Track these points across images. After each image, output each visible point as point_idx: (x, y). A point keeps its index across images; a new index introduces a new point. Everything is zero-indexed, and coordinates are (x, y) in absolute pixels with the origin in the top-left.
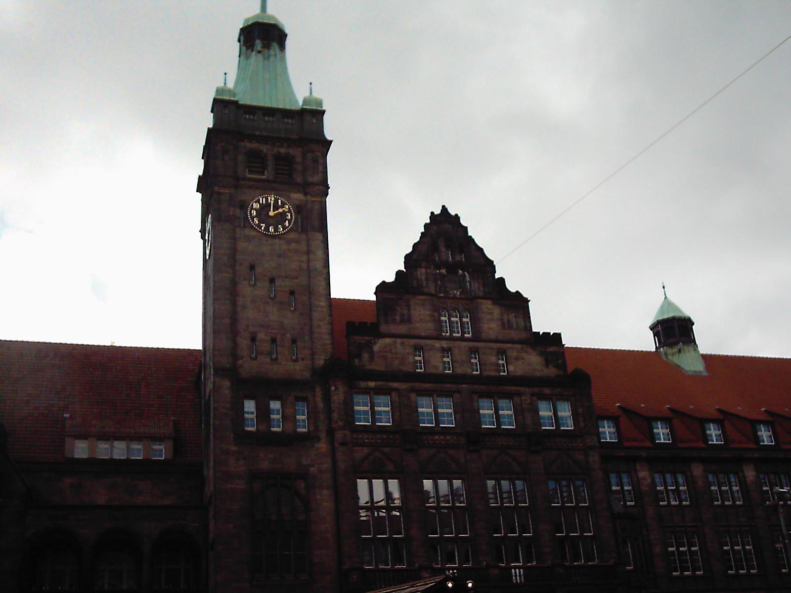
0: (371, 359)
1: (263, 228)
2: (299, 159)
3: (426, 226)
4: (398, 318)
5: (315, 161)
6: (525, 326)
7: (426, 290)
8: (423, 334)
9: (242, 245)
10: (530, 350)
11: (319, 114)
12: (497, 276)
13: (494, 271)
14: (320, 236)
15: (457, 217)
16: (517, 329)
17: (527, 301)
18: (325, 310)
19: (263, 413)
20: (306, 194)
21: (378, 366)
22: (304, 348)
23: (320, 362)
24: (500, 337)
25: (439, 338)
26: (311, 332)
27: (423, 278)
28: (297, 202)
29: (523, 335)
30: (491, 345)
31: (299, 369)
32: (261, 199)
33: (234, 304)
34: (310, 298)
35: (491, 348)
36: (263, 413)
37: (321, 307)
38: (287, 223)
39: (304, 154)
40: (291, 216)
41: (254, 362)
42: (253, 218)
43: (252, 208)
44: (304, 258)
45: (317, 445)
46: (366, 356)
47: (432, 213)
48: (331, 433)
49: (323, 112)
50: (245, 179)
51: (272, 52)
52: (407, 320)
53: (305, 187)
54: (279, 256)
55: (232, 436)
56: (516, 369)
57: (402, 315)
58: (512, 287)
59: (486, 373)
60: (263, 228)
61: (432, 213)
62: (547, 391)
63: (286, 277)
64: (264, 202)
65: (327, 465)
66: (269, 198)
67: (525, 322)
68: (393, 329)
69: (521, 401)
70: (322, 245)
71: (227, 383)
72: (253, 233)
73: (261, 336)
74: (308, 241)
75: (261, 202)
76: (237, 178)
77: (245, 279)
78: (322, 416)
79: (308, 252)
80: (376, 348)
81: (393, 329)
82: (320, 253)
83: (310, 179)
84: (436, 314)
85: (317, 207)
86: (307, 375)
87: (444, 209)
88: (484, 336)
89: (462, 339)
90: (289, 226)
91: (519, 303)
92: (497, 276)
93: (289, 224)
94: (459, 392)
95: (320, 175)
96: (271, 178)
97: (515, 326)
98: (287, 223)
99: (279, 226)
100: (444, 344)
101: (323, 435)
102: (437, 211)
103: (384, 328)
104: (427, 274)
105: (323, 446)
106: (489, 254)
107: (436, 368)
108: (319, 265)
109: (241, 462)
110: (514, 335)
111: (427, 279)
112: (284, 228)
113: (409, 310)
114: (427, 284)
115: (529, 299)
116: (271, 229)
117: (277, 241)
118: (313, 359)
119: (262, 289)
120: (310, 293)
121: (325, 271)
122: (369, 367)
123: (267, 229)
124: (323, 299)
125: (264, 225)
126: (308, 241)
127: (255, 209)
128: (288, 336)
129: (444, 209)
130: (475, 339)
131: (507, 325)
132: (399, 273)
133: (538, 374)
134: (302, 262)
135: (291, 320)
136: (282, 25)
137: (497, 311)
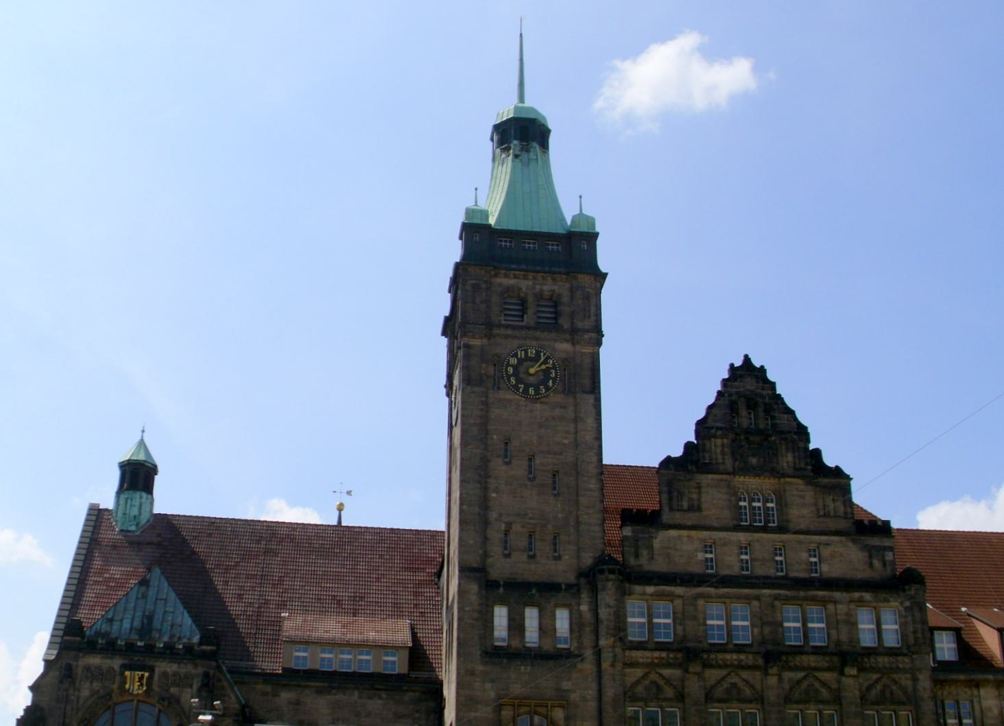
0: (652, 558)
1: (521, 390)
2: (565, 299)
3: (725, 382)
4: (685, 505)
5: (587, 297)
6: (846, 513)
8: (716, 524)
9: (495, 412)
10: (850, 544)
11: (592, 237)
12: (812, 446)
13: (807, 439)
14: (590, 399)
15: (762, 370)
16: (835, 516)
17: (848, 478)
18: (595, 494)
19: (517, 626)
20: (573, 344)
21: (660, 565)
22: (569, 543)
23: (588, 560)
24: (812, 528)
25: (737, 528)
26: (578, 523)
27: (719, 450)
28: (563, 355)
29: (843, 524)
30: (802, 537)
32: (519, 352)
33: (485, 489)
34: (577, 480)
35: (800, 542)
36: (517, 626)
37: (591, 490)
38: (550, 383)
39: (572, 290)
40: (556, 373)
41: (508, 560)
42: (509, 377)
43: (508, 365)
44: (571, 427)
45: (579, 666)
46: (645, 552)
47: (732, 365)
48: (598, 652)
49: (596, 235)
50: (500, 326)
51: (532, 155)
52: (696, 508)
53: (574, 334)
54: (541, 426)
55: (479, 653)
56: (828, 570)
57: (691, 499)
58: (829, 460)
59: (793, 574)
60: (521, 390)
61: (732, 365)
62: (867, 596)
63: (549, 452)
64: (523, 356)
65: (592, 692)
66: (529, 350)
67: (845, 506)
68: (678, 517)
69: (836, 609)
70: (593, 411)
72: (509, 396)
73: (517, 528)
74: (576, 406)
75: (519, 356)
76: (490, 325)
77: (499, 456)
78: (588, 629)
79: (576, 420)
80: (657, 543)
81: (678, 517)
82: (590, 421)
83: (580, 325)
84: (733, 498)
85: (588, 361)
86: (571, 578)
87: (747, 359)
89: (765, 529)
90: (553, 386)
91: (838, 481)
92: (812, 446)
93: (553, 383)
94: (758, 598)
95: (593, 318)
96: (532, 323)
97: (832, 513)
98: (550, 383)
99: (541, 387)
100: (742, 537)
101: (589, 653)
102: (738, 363)
103: (666, 517)
104: (723, 445)
105: (588, 666)
106: (802, 418)
108: (589, 437)
109: (488, 686)
111: (723, 453)
112: (547, 389)
113: (700, 493)
114: (724, 459)
115: (851, 477)
116: (531, 391)
117: (538, 406)
118: (578, 557)
119: (519, 468)
120: (577, 473)
121: (596, 444)
122: (647, 567)
123: (526, 391)
124: (594, 481)
125: (522, 386)
126: (576, 406)
127: (512, 366)
128: (550, 527)
129: (747, 359)
130: (781, 529)
132: (688, 446)
133: (859, 575)
134: (568, 432)
136: (544, 118)
137: (809, 494)
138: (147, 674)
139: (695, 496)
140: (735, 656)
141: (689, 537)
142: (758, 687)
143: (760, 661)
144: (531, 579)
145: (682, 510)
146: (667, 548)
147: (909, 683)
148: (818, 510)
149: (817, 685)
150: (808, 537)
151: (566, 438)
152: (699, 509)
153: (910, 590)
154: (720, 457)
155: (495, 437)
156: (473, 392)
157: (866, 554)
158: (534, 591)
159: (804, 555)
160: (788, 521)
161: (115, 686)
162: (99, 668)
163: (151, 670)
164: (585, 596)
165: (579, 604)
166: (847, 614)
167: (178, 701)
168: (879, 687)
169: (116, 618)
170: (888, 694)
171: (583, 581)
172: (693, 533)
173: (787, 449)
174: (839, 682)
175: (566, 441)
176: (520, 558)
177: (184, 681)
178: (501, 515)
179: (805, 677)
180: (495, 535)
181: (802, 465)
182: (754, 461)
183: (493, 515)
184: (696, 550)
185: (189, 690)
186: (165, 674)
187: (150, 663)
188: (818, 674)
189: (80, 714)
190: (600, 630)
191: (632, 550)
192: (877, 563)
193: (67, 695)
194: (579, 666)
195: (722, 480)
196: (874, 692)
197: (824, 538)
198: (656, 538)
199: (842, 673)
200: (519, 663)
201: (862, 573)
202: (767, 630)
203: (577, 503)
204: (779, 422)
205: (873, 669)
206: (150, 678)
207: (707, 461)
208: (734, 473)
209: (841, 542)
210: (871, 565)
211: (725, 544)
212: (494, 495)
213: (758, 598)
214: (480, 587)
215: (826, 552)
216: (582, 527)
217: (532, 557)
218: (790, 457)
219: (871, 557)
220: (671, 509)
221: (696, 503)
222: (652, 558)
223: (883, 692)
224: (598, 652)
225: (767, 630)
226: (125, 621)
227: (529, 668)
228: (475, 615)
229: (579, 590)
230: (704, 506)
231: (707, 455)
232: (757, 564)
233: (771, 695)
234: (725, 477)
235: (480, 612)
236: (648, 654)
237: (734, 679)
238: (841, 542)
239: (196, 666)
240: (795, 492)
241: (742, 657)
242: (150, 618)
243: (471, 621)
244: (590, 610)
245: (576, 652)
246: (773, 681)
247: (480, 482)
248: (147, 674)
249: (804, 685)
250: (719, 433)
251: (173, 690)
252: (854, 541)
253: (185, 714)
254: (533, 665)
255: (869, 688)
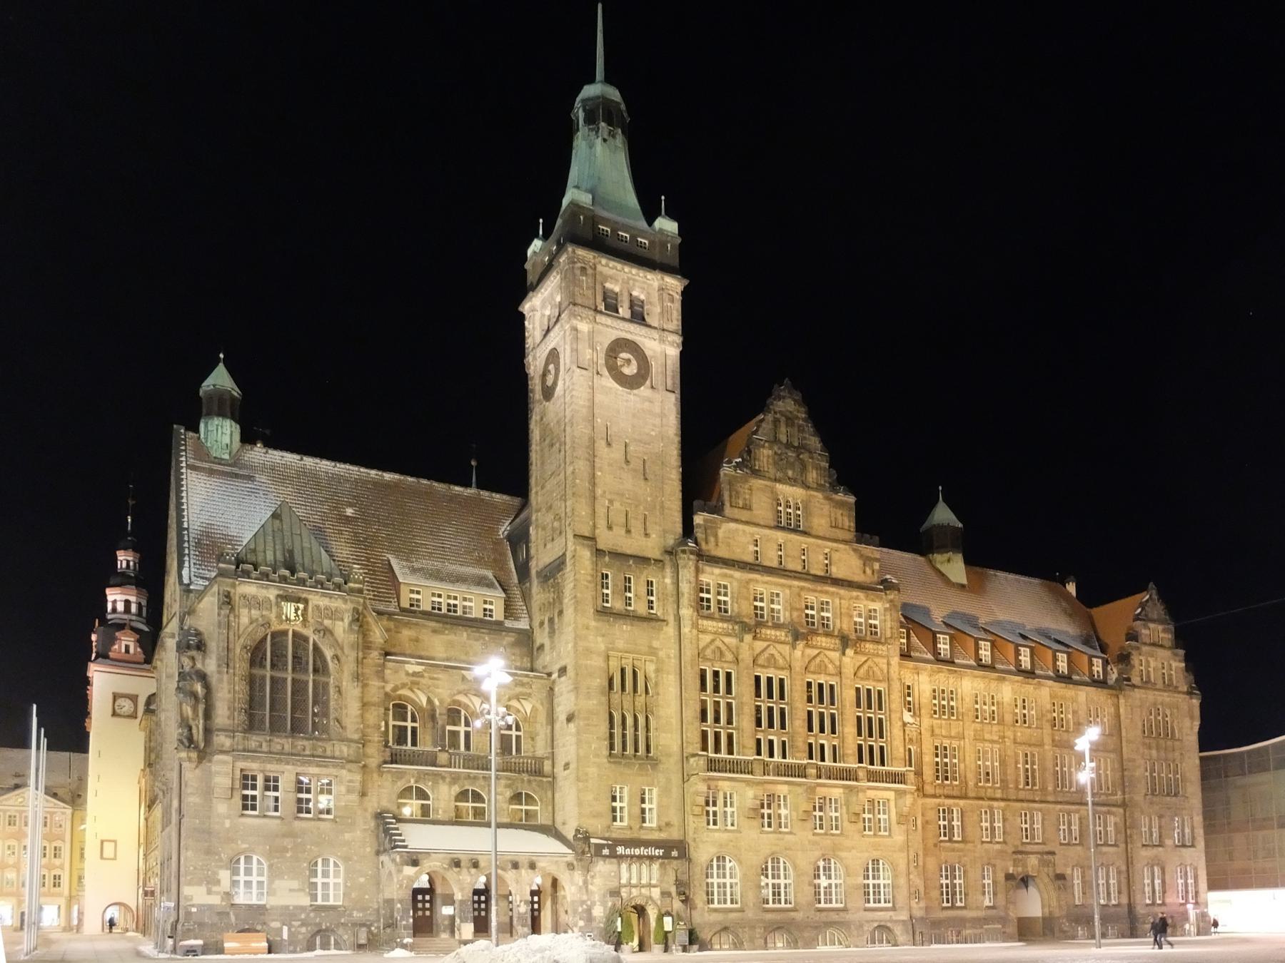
4: (741, 503)
7: (767, 475)
8: (762, 523)
9: (599, 398)
16: (842, 529)
21: (722, 552)
24: (828, 536)
26: (662, 507)
27: (765, 460)
30: (820, 542)
31: (651, 546)
35: (818, 546)
37: (672, 480)
41: (611, 533)
46: (712, 539)
52: (747, 507)
57: (745, 499)
71: (586, 554)
73: (617, 505)
78: (671, 599)
80: (721, 533)
81: (736, 513)
86: (655, 553)
88: (814, 533)
97: (840, 526)
100: (781, 536)
101: (671, 619)
103: (728, 510)
107: (771, 560)
110: (840, 534)
113: (751, 494)
119: (617, 454)
130: (805, 533)
131: (834, 525)
134: (654, 425)
135: (644, 491)
137: (827, 507)
138: (301, 606)
139: (747, 497)
140: (773, 632)
141: (744, 531)
142: (788, 658)
143: (790, 639)
144: (629, 552)
145: (739, 508)
146: (729, 538)
147: (885, 667)
148: (831, 522)
149: (826, 660)
150: (824, 542)
151: (653, 430)
152: (750, 509)
153: (891, 594)
154: (766, 465)
155: (599, 420)
156: (582, 375)
157: (862, 562)
158: (631, 562)
159: (821, 557)
160: (812, 528)
161: (273, 616)
162: (254, 597)
163: (306, 601)
164: (668, 571)
165: (664, 577)
166: (848, 608)
167: (331, 633)
168: (865, 667)
169: (257, 549)
170: (871, 673)
171: (667, 557)
172: (747, 528)
173: (812, 468)
174: (840, 661)
175: (653, 433)
176: (619, 531)
177: (334, 615)
178: (605, 492)
179: (818, 654)
180: (601, 511)
181: (823, 482)
182: (790, 473)
183: (599, 492)
184: (748, 543)
185: (341, 623)
186: (318, 607)
187: (304, 596)
188: (828, 653)
189: (242, 640)
190: (681, 601)
191: (704, 536)
192: (868, 571)
193: (228, 621)
194: (664, 628)
195: (766, 486)
196: (862, 671)
197: (835, 545)
198: (720, 528)
199: (844, 654)
200: (621, 622)
201: (858, 577)
202: (795, 614)
203: (662, 489)
204: (809, 443)
205: (864, 654)
206: (305, 609)
207: (757, 468)
208: (776, 480)
209: (845, 550)
210: (864, 572)
211: (768, 540)
212: (599, 474)
213: (790, 587)
214: (592, 554)
215: (835, 556)
216: (666, 511)
217: (628, 531)
218: (815, 475)
219: (864, 565)
220: (731, 506)
221: (748, 502)
222: (717, 545)
223: (868, 671)
224: (678, 619)
225: (795, 614)
226: (268, 552)
227: (629, 628)
228: (589, 578)
229: (664, 565)
230: (754, 506)
231: (757, 463)
232: (789, 559)
233: (798, 666)
234: (768, 483)
235: (592, 576)
236: (715, 624)
237: (772, 650)
238: (845, 550)
239: (345, 601)
240: (817, 504)
241: (778, 633)
242: (291, 552)
243: (586, 583)
244: (673, 583)
245: (662, 618)
246: (798, 653)
247: (589, 460)
248: (301, 606)
249: (818, 660)
250: (767, 444)
251: (327, 622)
252: (855, 550)
253: (339, 645)
254: (632, 625)
255: (859, 667)
